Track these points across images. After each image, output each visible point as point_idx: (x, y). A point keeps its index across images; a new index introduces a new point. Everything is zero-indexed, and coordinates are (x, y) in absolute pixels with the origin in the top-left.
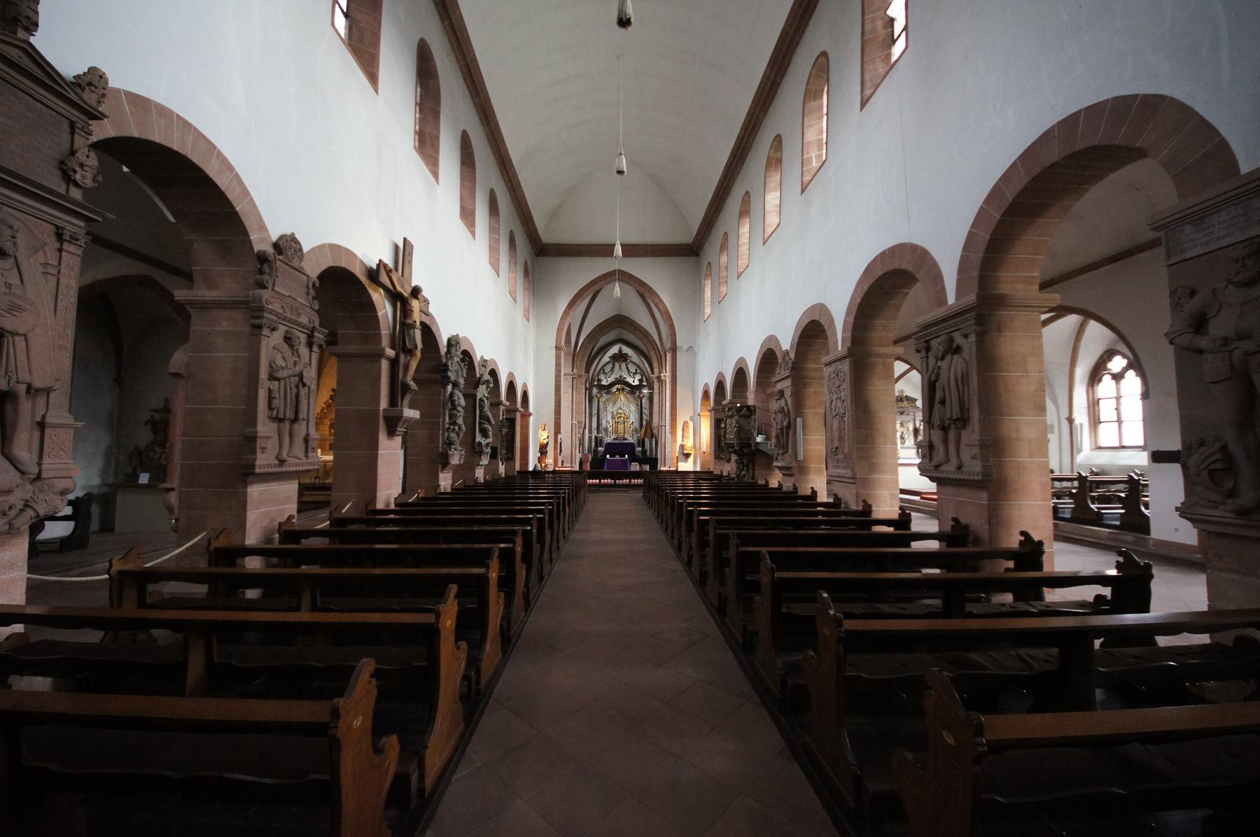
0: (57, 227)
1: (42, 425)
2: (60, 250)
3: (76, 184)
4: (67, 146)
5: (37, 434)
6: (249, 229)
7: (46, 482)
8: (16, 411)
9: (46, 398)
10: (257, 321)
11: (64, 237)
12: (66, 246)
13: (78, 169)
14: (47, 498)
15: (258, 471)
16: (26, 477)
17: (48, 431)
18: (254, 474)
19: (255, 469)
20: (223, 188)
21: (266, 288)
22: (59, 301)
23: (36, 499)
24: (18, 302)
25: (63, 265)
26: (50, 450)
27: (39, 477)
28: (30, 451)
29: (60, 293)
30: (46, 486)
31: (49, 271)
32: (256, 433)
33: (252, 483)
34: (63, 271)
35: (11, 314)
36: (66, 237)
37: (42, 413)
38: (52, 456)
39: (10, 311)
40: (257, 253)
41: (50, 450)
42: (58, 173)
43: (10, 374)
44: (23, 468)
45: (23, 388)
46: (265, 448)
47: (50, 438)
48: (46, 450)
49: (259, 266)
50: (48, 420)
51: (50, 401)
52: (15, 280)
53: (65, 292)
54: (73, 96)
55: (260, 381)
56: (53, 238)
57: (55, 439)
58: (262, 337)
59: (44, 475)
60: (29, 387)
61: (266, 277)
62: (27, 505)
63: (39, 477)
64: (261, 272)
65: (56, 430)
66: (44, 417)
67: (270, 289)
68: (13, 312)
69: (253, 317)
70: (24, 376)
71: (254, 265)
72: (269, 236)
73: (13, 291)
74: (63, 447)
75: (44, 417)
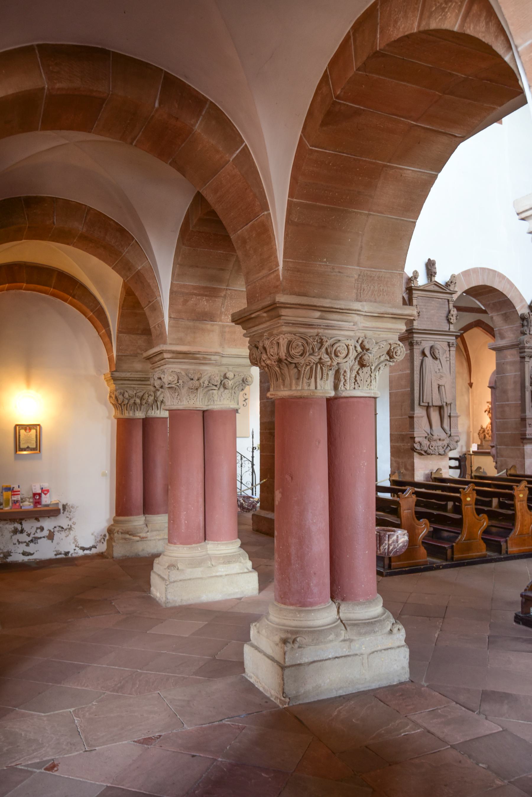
0: (449, 343)
1: (450, 417)
2: (450, 351)
3: (451, 323)
4: (447, 309)
5: (449, 420)
6: (515, 305)
8: (444, 412)
10: (522, 355)
13: (452, 318)
15: (528, 437)
17: (452, 419)
18: (526, 439)
19: (526, 436)
20: (501, 290)
21: (526, 334)
27: (450, 436)
28: (447, 426)
32: (526, 416)
33: (526, 443)
36: (451, 345)
37: (449, 412)
40: (521, 315)
42: (446, 321)
44: (447, 432)
45: (445, 404)
46: (530, 424)
48: (452, 426)
49: (522, 322)
50: (452, 415)
52: (440, 367)
54: (448, 291)
55: (526, 387)
56: (448, 347)
58: (525, 363)
59: (452, 435)
60: (446, 403)
61: (526, 328)
62: (448, 445)
63: (450, 436)
64: (523, 326)
66: (450, 413)
67: (528, 334)
69: (520, 353)
70: (445, 400)
71: (519, 323)
72: (526, 302)
75: (450, 413)
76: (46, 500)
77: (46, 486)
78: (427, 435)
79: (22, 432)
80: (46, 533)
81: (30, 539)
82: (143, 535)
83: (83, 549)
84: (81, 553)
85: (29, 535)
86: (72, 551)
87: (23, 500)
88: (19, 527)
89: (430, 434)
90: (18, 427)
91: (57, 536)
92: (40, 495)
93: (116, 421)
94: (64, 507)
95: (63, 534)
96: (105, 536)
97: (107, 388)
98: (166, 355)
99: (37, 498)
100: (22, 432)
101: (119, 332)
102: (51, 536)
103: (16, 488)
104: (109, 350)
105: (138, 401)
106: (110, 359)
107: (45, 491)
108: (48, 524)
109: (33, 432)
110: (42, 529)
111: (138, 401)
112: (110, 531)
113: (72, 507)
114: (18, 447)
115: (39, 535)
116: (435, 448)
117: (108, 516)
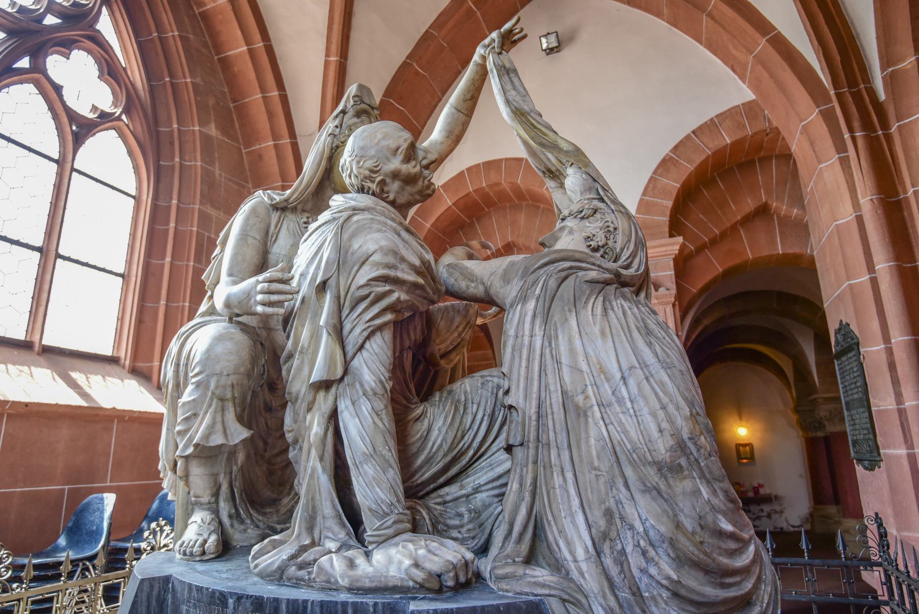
76: (762, 491)
77: (761, 482)
79: (741, 448)
80: (765, 514)
81: (754, 517)
82: (836, 519)
83: (794, 527)
84: (792, 529)
85: (754, 514)
86: (785, 528)
87: (747, 491)
88: (747, 508)
90: (738, 446)
91: (774, 516)
92: (757, 488)
93: (803, 439)
94: (776, 497)
95: (777, 516)
96: (808, 519)
97: (794, 417)
98: (819, 400)
99: (756, 490)
100: (741, 448)
101: (795, 381)
102: (769, 516)
103: (742, 483)
104: (791, 393)
105: (817, 425)
106: (792, 398)
107: (761, 486)
108: (766, 508)
109: (748, 448)
110: (762, 511)
111: (817, 425)
112: (811, 515)
113: (781, 497)
114: (739, 457)
115: (761, 514)
117: (808, 505)
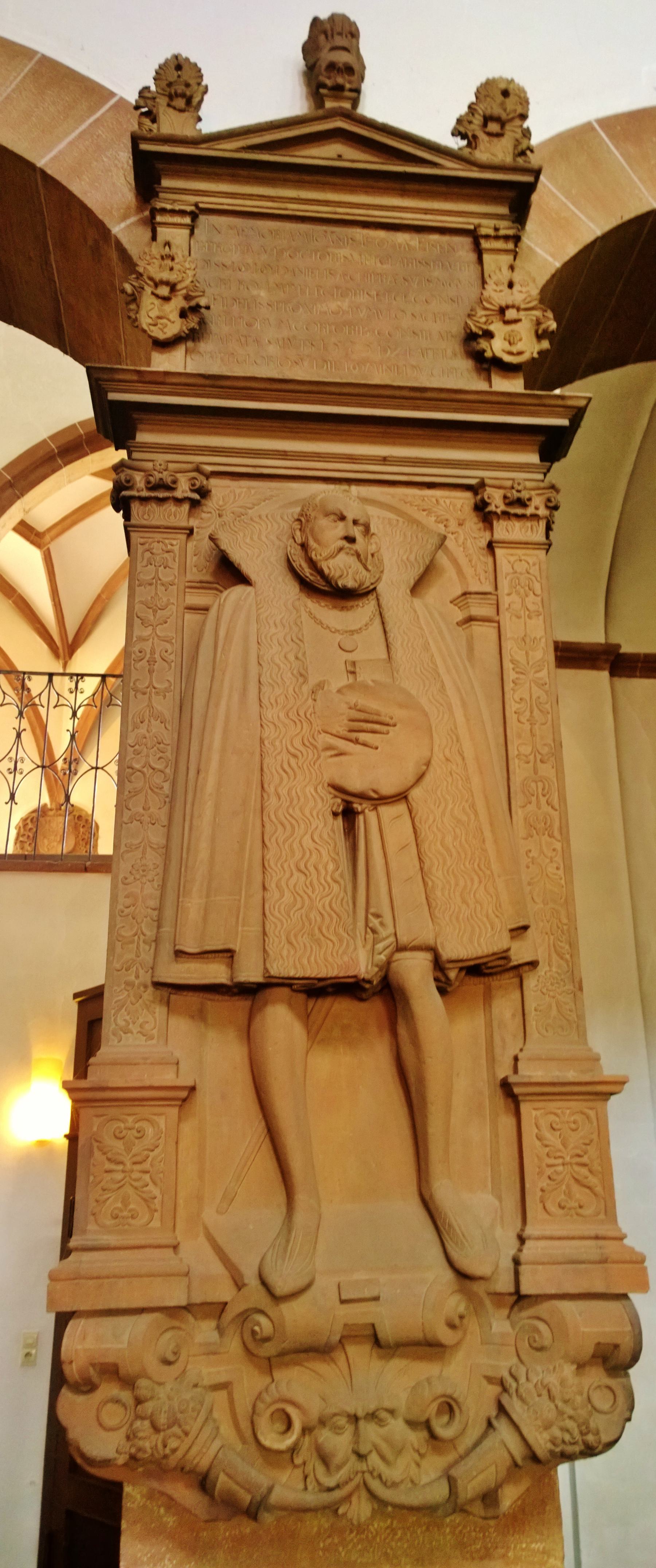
7: (543, 1308)
9: (517, 995)
11: (492, 508)
12: (503, 530)
14: (552, 1380)
16: (479, 1288)
22: (509, 686)
23: (523, 1380)
24: (373, 704)
25: (504, 584)
26: (544, 1183)
29: (508, 665)
30: (542, 1326)
31: (476, 611)
34: (505, 601)
35: (356, 741)
38: (552, 1208)
39: (354, 735)
41: (544, 1183)
43: (374, 922)
47: (539, 1138)
51: (530, 1005)
53: (520, 656)
57: (552, 1139)
60: (438, 964)
65: (553, 1106)
68: (362, 737)
73: (364, 676)
74: (584, 1171)
78: (224, 1292)
89: (252, 1281)
116: (325, 1436)
